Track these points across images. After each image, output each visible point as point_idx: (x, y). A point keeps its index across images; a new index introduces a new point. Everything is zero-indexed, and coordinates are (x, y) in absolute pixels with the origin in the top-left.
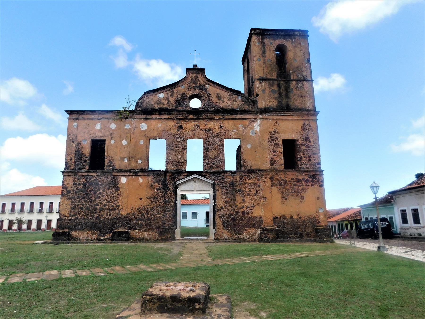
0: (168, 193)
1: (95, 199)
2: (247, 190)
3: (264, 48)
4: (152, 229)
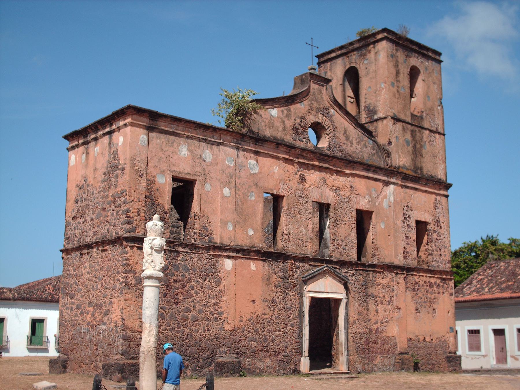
2: (381, 296)
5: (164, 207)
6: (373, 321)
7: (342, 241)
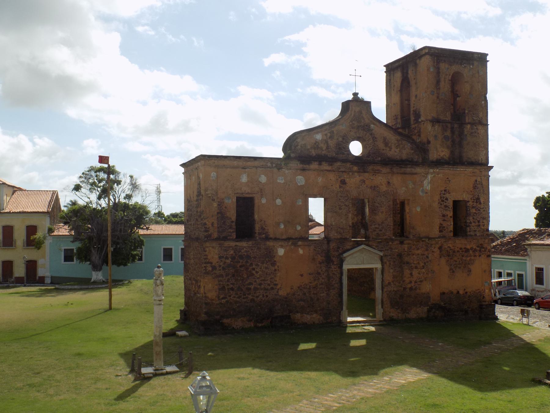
0: (333, 267)
2: (415, 262)
3: (439, 76)
4: (316, 312)
5: (231, 219)
7: (379, 225)
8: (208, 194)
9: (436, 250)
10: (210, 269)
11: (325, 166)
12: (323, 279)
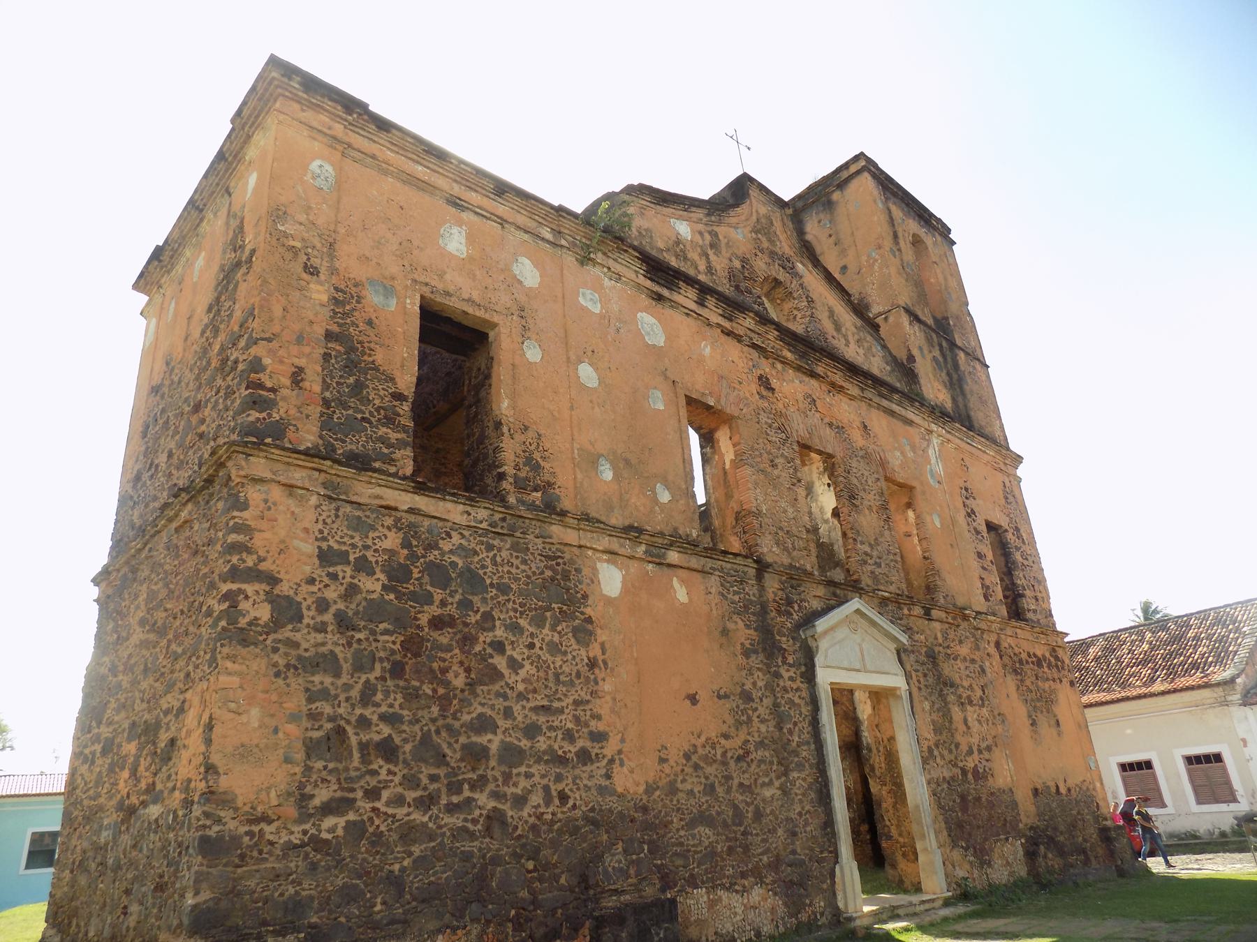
1: (471, 685)
2: (966, 684)
4: (757, 874)
6: (964, 748)
8: (286, 235)
9: (992, 649)
10: (264, 613)
11: (713, 313)
12: (762, 721)
